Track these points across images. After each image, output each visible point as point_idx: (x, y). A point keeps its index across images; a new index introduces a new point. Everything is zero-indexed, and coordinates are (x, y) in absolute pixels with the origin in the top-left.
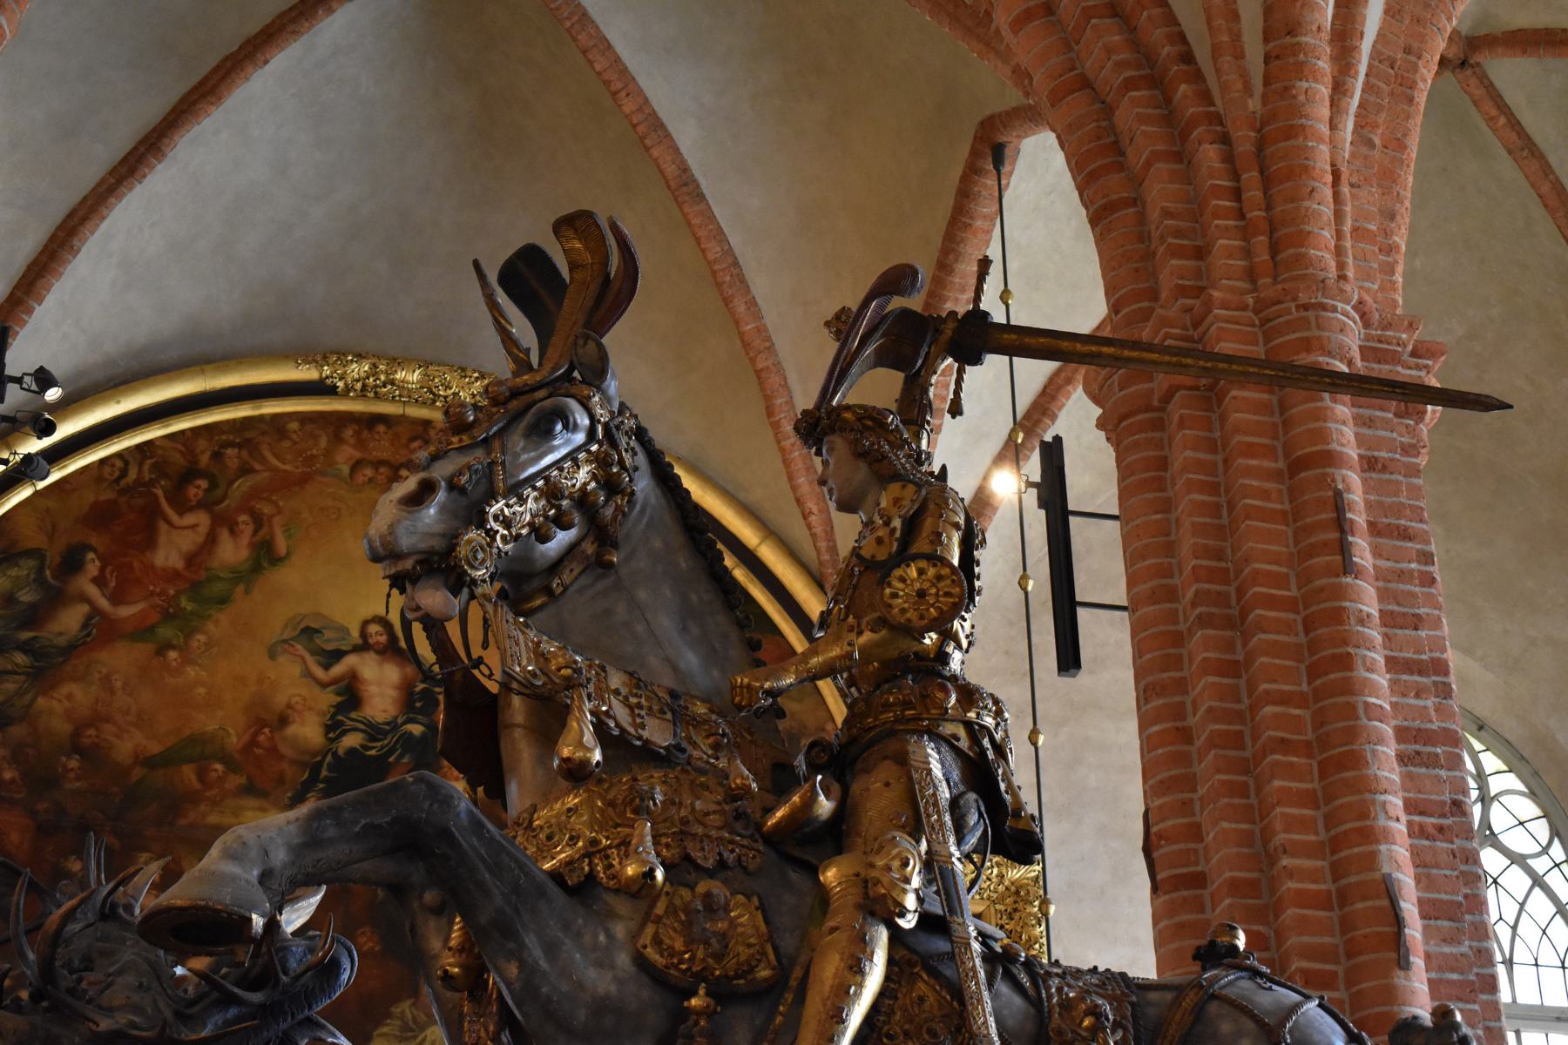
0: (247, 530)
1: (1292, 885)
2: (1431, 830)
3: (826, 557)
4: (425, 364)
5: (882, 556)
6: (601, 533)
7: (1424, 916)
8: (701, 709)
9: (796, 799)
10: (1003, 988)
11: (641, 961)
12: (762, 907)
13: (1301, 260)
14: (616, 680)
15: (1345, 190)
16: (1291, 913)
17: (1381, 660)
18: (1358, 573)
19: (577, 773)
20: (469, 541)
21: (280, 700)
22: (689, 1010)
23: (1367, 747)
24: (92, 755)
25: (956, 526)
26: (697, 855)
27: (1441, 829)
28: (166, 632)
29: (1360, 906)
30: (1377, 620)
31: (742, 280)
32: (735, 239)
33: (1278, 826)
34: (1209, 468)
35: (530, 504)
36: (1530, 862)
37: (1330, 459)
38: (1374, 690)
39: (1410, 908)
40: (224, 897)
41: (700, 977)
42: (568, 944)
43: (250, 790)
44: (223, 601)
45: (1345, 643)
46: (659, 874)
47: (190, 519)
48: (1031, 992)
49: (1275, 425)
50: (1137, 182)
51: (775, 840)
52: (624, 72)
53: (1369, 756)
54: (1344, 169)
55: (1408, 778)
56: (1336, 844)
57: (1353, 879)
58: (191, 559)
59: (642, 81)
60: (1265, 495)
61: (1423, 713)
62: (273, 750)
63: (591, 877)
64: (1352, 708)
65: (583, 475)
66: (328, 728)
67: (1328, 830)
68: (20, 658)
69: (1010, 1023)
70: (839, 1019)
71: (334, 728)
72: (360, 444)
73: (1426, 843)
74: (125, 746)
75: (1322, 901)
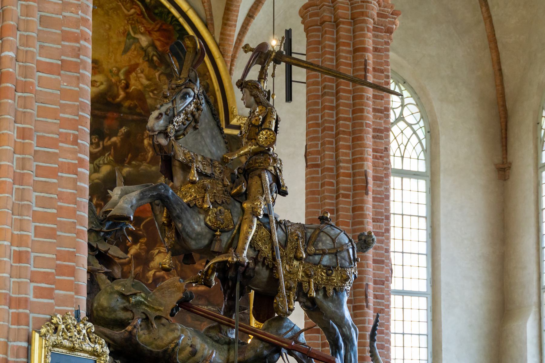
1: (342, 171)
2: (378, 157)
3: (209, 17)
5: (257, 124)
7: (374, 180)
9: (238, 188)
10: (279, 230)
11: (206, 224)
12: (231, 212)
19: (193, 182)
20: (170, 128)
22: (216, 235)
23: (365, 135)
25: (274, 119)
26: (218, 201)
27: (381, 157)
29: (358, 178)
30: (371, 98)
33: (340, 155)
35: (182, 117)
36: (413, 126)
38: (368, 119)
39: (370, 179)
41: (218, 228)
42: (192, 221)
45: (362, 105)
46: (211, 207)
48: (285, 230)
49: (351, 36)
51: (234, 196)
53: (365, 138)
55: (374, 142)
56: (354, 160)
57: (357, 171)
61: (380, 124)
64: (362, 123)
67: (352, 156)
69: (280, 238)
70: (247, 238)
73: (377, 160)
75: (348, 175)
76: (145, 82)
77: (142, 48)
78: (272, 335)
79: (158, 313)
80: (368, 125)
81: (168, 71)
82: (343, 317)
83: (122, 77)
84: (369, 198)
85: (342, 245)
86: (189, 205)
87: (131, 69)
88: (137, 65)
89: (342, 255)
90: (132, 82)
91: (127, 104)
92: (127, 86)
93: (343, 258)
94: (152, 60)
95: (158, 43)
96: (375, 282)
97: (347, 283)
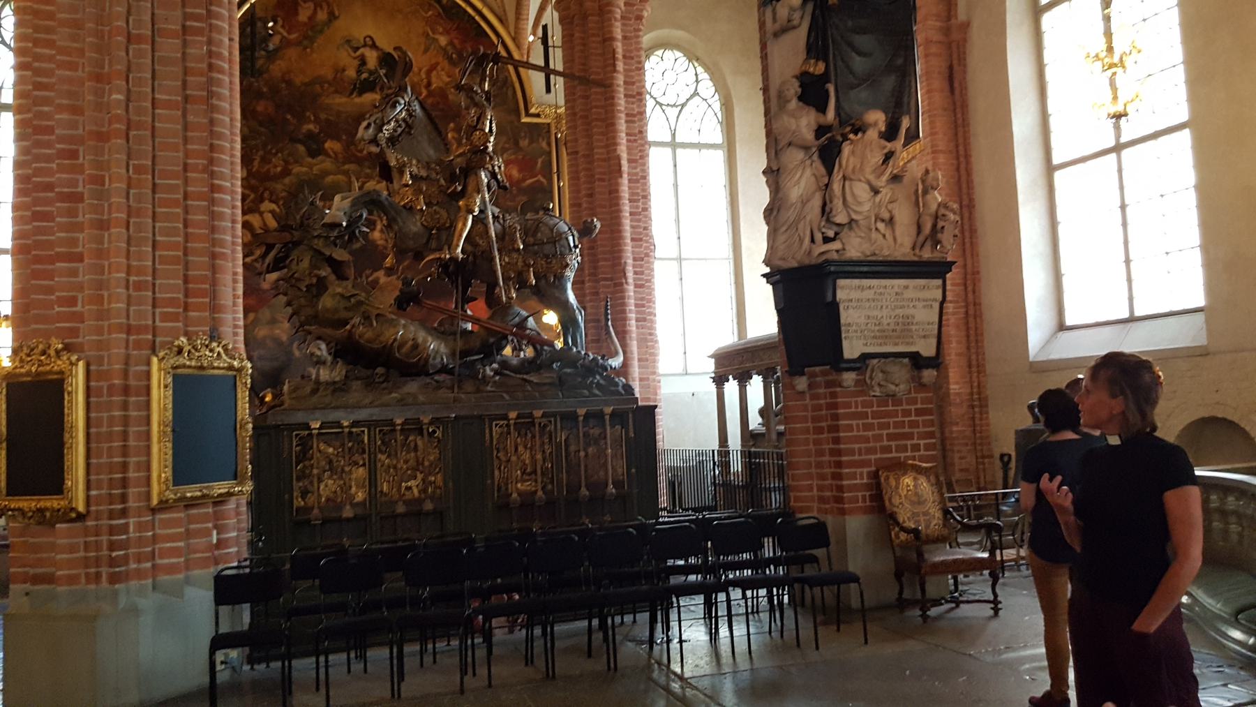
6: (409, 126)
8: (433, 165)
10: (496, 224)
14: (414, 162)
19: (407, 185)
24: (289, 83)
28: (305, 43)
37: (612, 39)
38: (620, 105)
39: (624, 163)
40: (337, 220)
43: (336, 92)
44: (321, 32)
47: (307, 5)
51: (449, 195)
58: (310, 18)
61: (633, 109)
62: (342, 79)
63: (411, 207)
66: (358, 72)
68: (263, 53)
70: (461, 236)
71: (359, 72)
74: (298, 80)
75: (604, 160)
76: (447, 80)
77: (441, 47)
78: (496, 325)
79: (378, 312)
80: (620, 111)
82: (567, 301)
83: (424, 76)
84: (625, 181)
87: (433, 68)
88: (437, 64)
89: (562, 243)
90: (434, 79)
92: (429, 84)
93: (562, 246)
95: (456, 42)
96: (635, 259)
97: (568, 269)
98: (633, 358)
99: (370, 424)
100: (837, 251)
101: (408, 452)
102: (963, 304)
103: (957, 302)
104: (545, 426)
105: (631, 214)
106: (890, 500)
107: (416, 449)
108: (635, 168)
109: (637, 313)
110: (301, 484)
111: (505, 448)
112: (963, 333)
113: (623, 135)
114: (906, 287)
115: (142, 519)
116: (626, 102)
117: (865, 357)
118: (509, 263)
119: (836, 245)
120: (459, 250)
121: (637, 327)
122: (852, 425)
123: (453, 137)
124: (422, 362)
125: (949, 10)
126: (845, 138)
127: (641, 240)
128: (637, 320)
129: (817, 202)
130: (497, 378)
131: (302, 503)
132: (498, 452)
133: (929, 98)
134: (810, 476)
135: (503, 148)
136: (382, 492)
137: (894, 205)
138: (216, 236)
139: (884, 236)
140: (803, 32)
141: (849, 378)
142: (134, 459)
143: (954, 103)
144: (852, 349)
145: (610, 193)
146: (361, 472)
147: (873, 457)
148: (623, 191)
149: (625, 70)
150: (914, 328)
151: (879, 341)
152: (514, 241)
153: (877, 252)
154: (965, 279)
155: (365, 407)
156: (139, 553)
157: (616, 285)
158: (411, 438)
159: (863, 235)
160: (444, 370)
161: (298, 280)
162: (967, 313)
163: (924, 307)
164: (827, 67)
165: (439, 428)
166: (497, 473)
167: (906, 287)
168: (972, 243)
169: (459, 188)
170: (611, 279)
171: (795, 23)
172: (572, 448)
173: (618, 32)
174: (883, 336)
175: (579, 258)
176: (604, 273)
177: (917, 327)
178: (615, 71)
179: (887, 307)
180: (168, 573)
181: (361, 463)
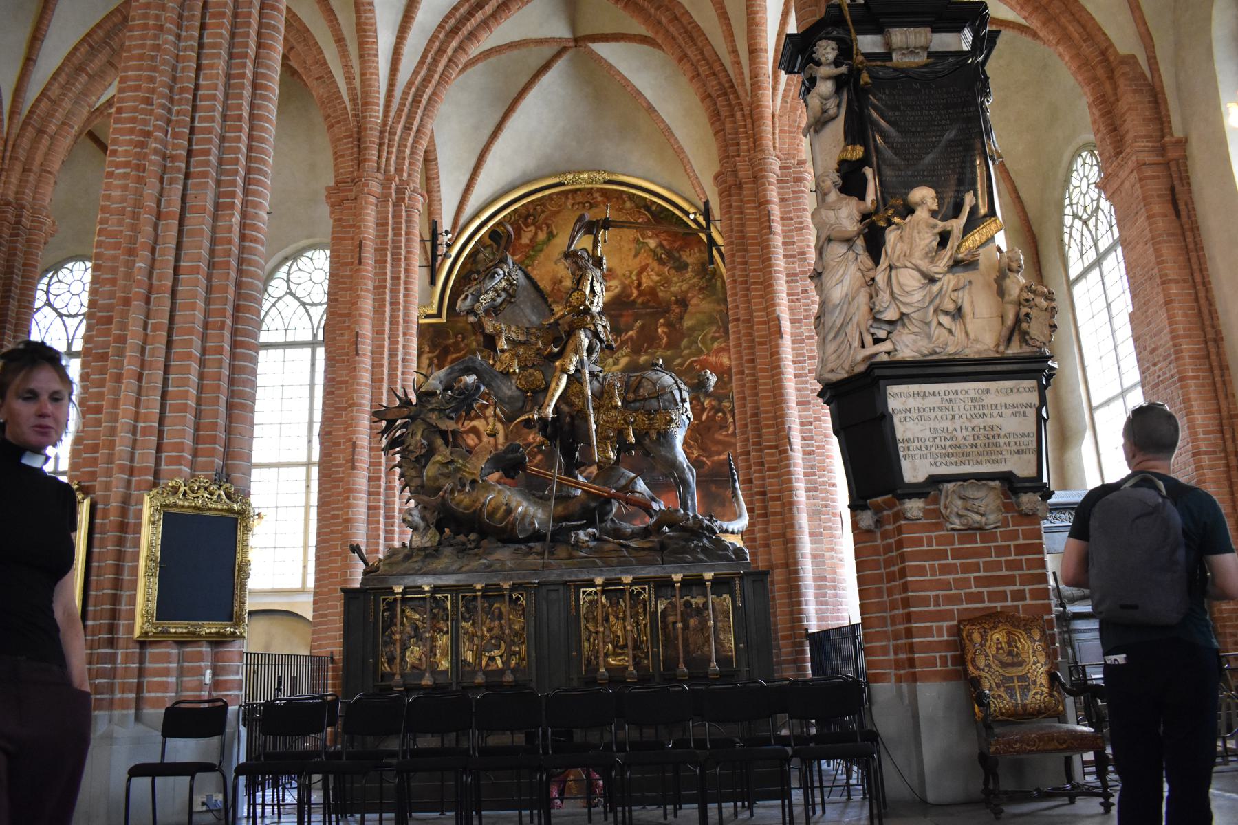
0: (545, 228)
4: (588, 172)
6: (510, 295)
8: (534, 330)
10: (595, 383)
11: (517, 388)
13: (761, 145)
14: (513, 328)
15: (776, 120)
16: (756, 327)
17: (781, 257)
18: (774, 233)
21: (560, 276)
28: (527, 262)
31: (672, 133)
32: (667, 121)
34: (740, 207)
37: (767, 202)
38: (778, 265)
40: (431, 388)
44: (541, 250)
47: (529, 229)
50: (723, 124)
51: (546, 357)
52: (625, 79)
54: (777, 113)
55: (789, 288)
58: (531, 240)
59: (633, 81)
60: (752, 214)
61: (794, 269)
62: (559, 290)
65: (504, 284)
69: (595, 389)
70: (553, 396)
72: (574, 198)
75: (765, 323)
76: (656, 278)
79: (473, 477)
80: (779, 272)
81: (677, 263)
85: (663, 388)
86: (502, 372)
87: (643, 270)
88: (647, 265)
91: (640, 300)
92: (640, 284)
94: (661, 258)
95: (665, 243)
96: (802, 424)
97: (674, 425)
98: (802, 532)
99: (454, 589)
100: (888, 353)
101: (492, 620)
102: (1222, 455)
103: (1214, 453)
104: (639, 593)
105: (796, 376)
106: (973, 661)
107: (500, 617)
108: (799, 328)
109: (808, 482)
110: (388, 650)
111: (595, 619)
112: (1227, 490)
113: (784, 295)
114: (987, 391)
115: (129, 651)
116: (787, 263)
117: (935, 481)
118: (607, 422)
119: (887, 346)
120: (550, 409)
121: (808, 498)
122: (924, 567)
123: (663, 332)
124: (509, 526)
125: (1162, 130)
126: (890, 223)
127: (809, 403)
128: (808, 490)
129: (862, 298)
130: (594, 544)
131: (388, 669)
132: (588, 622)
133: (1150, 224)
134: (884, 635)
135: (713, 337)
136: (465, 661)
137: (961, 293)
138: (235, 388)
139: (950, 331)
140: (840, 121)
141: (914, 507)
142: (127, 593)
143: (1182, 226)
144: (914, 470)
145: (771, 355)
146: (443, 641)
147: (955, 607)
148: (785, 352)
149: (783, 231)
150: (1002, 441)
151: (953, 459)
152: (612, 398)
153: (938, 350)
154: (1221, 425)
155: (454, 573)
156: (124, 683)
157: (781, 452)
158: (495, 606)
159: (917, 330)
160: (537, 536)
161: (412, 452)
162: (1228, 465)
163: (1014, 415)
164: (866, 151)
165: (522, 595)
166: (586, 645)
167: (987, 391)
168: (1224, 383)
169: (556, 350)
170: (776, 447)
171: (832, 112)
172: (671, 619)
173: (773, 194)
174: (960, 453)
175: (690, 414)
176: (769, 441)
177: (1006, 440)
178: (771, 232)
179: (961, 417)
180: (154, 707)
181: (445, 629)
